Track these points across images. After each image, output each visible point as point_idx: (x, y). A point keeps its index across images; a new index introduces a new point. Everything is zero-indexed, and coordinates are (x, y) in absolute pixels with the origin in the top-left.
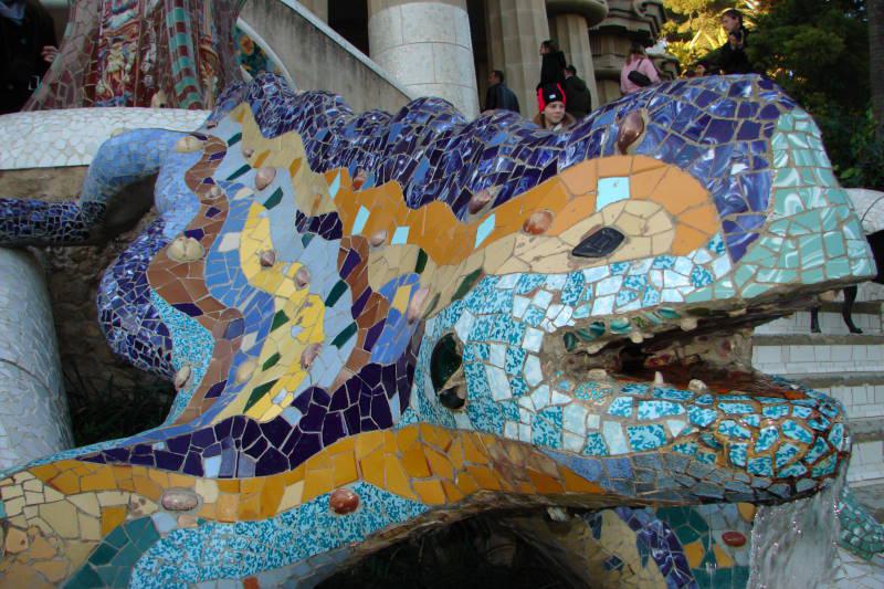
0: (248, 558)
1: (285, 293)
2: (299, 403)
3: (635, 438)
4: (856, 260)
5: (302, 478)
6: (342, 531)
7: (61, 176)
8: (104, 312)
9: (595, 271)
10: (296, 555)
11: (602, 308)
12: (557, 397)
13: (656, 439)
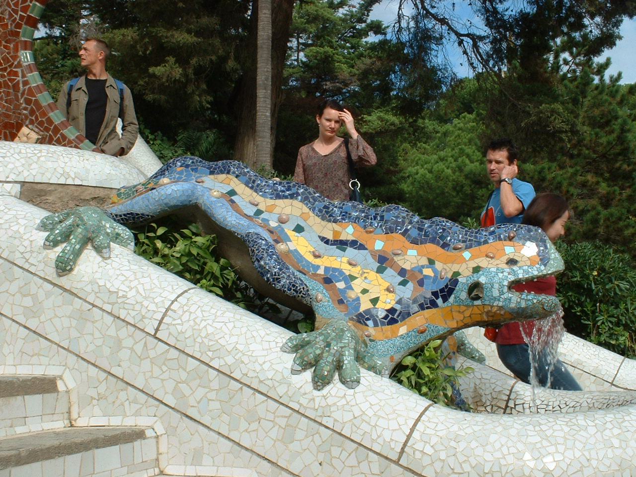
1: (347, 269)
2: (399, 302)
7: (60, 189)
8: (275, 272)
9: (515, 268)
11: (521, 276)
12: (510, 295)
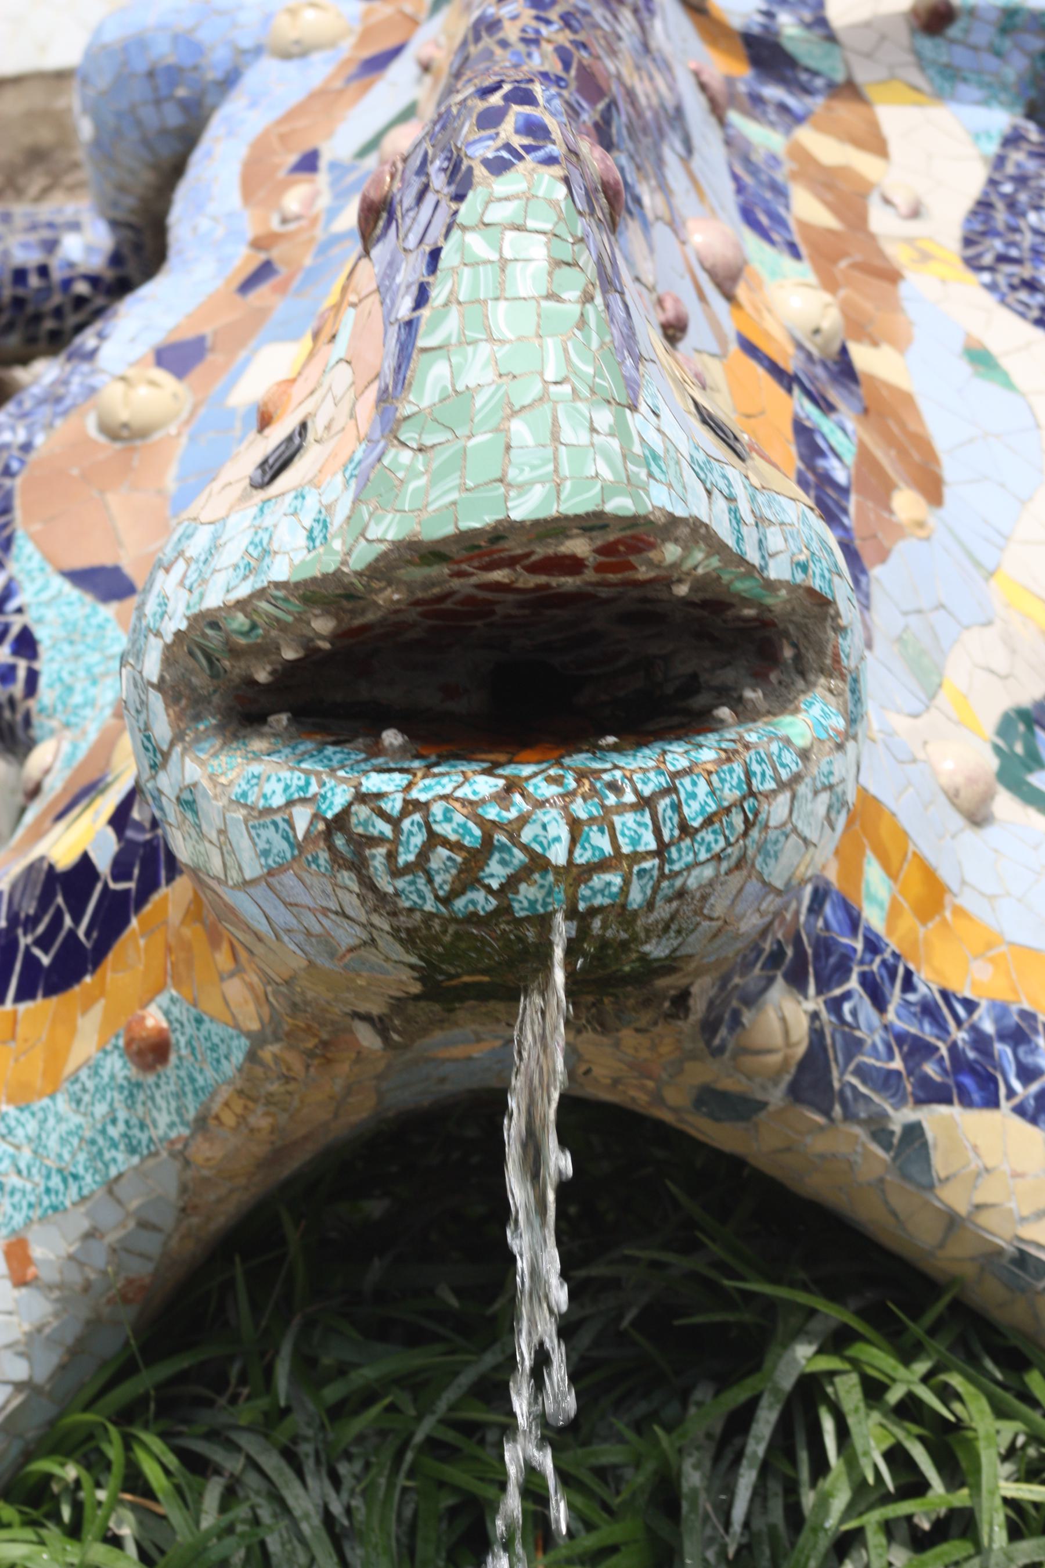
0: (12, 1193)
3: (262, 845)
4: (523, 488)
5: (102, 993)
6: (155, 1113)
10: (89, 1179)
13: (285, 845)
